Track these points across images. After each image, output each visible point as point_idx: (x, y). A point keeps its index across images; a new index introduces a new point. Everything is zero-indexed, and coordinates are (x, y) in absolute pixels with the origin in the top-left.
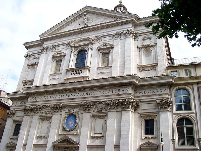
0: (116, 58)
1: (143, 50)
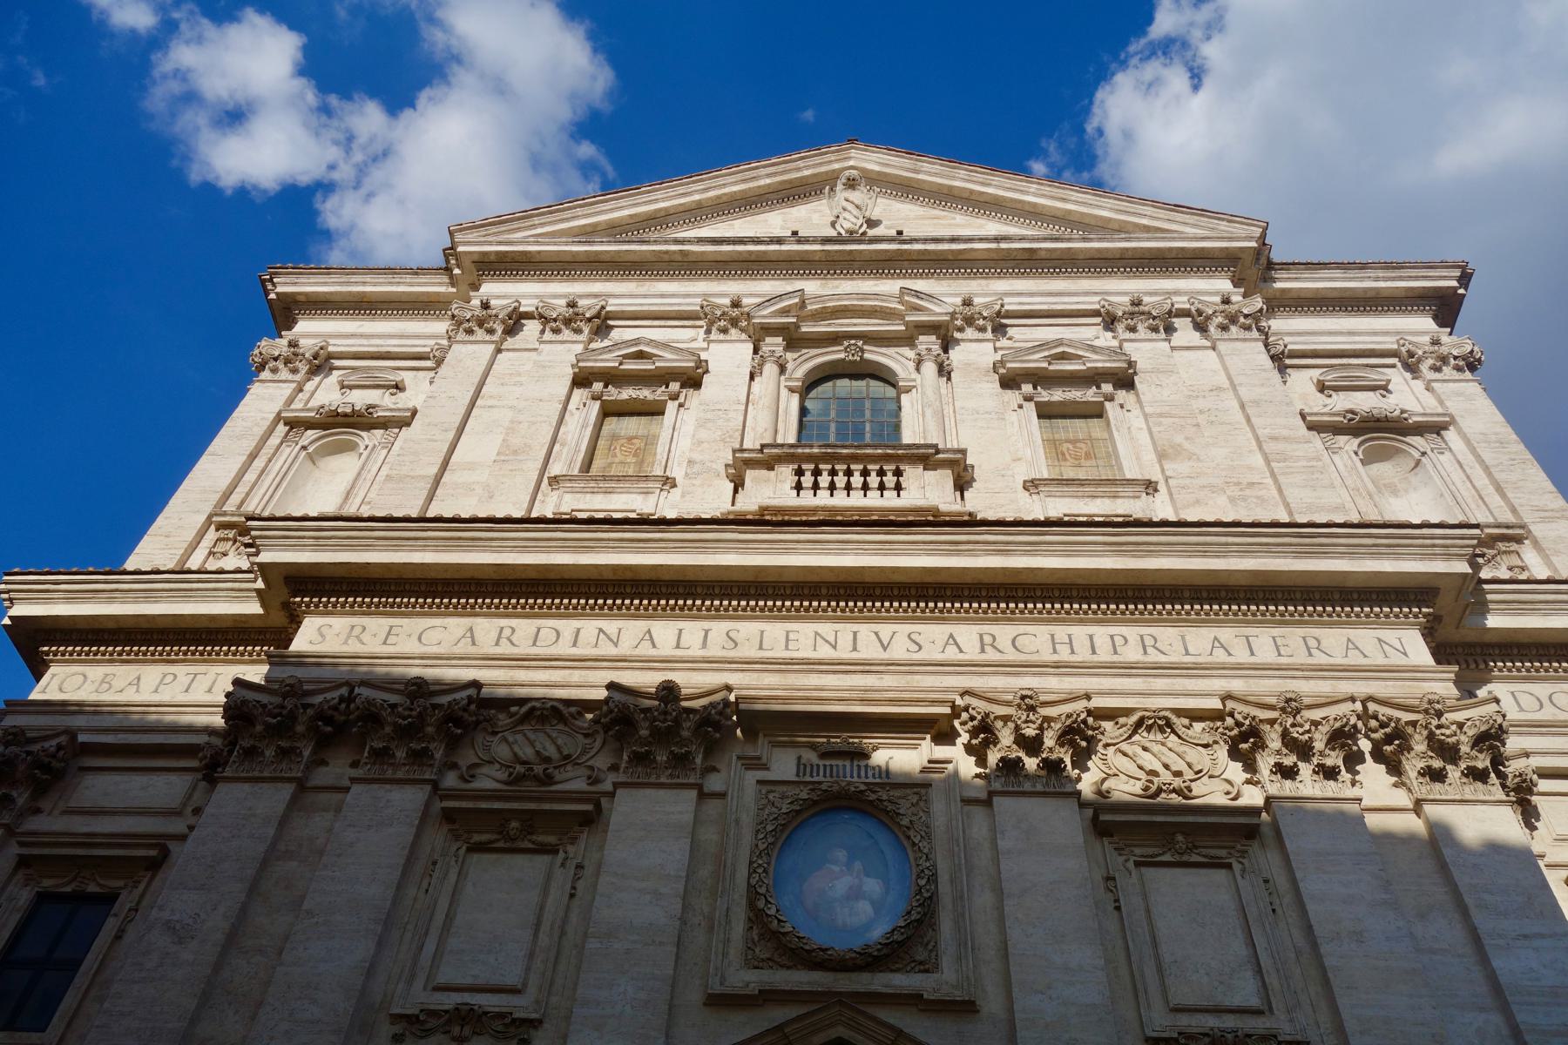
0: (1179, 439)
1: (1349, 444)
